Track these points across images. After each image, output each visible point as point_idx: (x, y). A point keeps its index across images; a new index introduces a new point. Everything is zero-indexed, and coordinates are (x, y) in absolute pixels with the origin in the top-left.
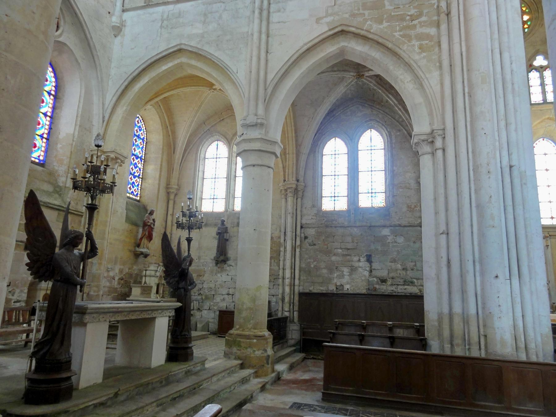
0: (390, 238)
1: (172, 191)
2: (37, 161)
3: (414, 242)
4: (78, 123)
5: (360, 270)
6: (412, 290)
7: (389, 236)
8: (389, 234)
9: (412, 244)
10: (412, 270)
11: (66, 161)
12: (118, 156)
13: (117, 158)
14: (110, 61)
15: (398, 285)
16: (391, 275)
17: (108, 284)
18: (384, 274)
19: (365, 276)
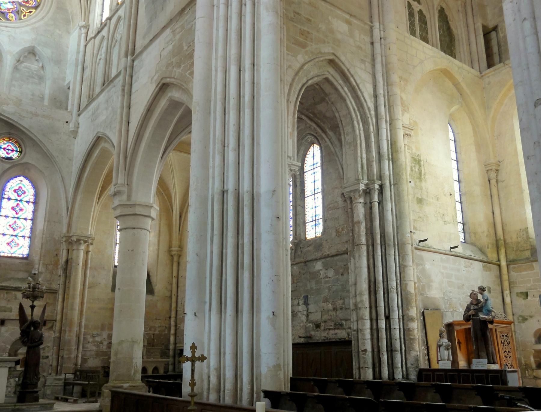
0: (321, 272)
1: (173, 253)
2: (21, 256)
3: (342, 275)
4: (47, 219)
5: (299, 314)
6: (342, 334)
7: (321, 270)
8: (321, 268)
9: (340, 277)
10: (341, 309)
11: (39, 252)
12: (78, 238)
13: (78, 241)
14: (70, 160)
15: (330, 329)
16: (325, 317)
17: (94, 348)
18: (316, 317)
19: (303, 321)
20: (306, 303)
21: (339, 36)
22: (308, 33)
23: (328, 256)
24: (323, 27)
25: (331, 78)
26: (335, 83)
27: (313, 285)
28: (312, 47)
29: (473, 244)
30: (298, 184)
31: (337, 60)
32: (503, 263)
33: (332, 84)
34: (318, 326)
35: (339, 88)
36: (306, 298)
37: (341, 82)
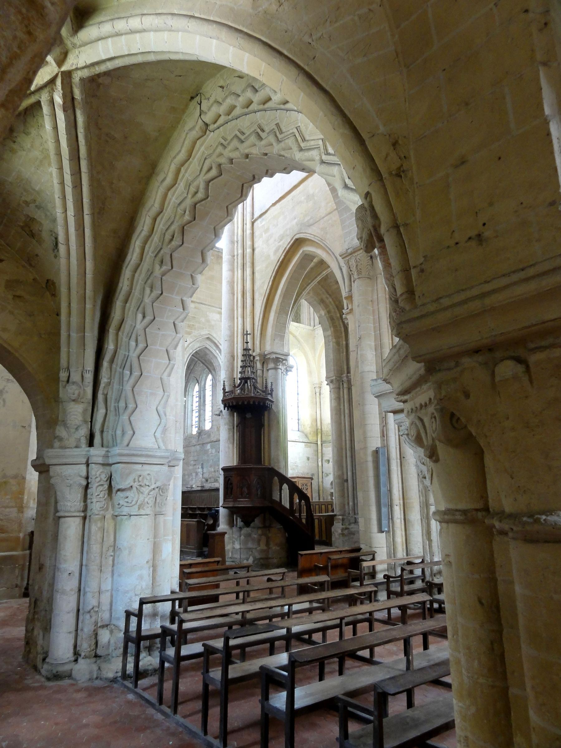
0: (210, 450)
16: (210, 476)
18: (206, 476)
20: (202, 468)
21: (213, 323)
22: (193, 325)
23: (213, 442)
24: (203, 320)
25: (208, 346)
26: (211, 349)
27: (205, 457)
28: (195, 333)
29: (303, 432)
30: (202, 397)
31: (211, 337)
32: (319, 443)
33: (209, 350)
34: (207, 481)
35: (213, 352)
36: (202, 464)
37: (215, 348)
